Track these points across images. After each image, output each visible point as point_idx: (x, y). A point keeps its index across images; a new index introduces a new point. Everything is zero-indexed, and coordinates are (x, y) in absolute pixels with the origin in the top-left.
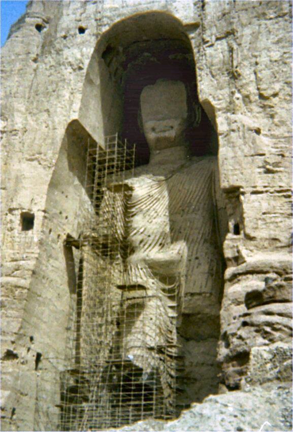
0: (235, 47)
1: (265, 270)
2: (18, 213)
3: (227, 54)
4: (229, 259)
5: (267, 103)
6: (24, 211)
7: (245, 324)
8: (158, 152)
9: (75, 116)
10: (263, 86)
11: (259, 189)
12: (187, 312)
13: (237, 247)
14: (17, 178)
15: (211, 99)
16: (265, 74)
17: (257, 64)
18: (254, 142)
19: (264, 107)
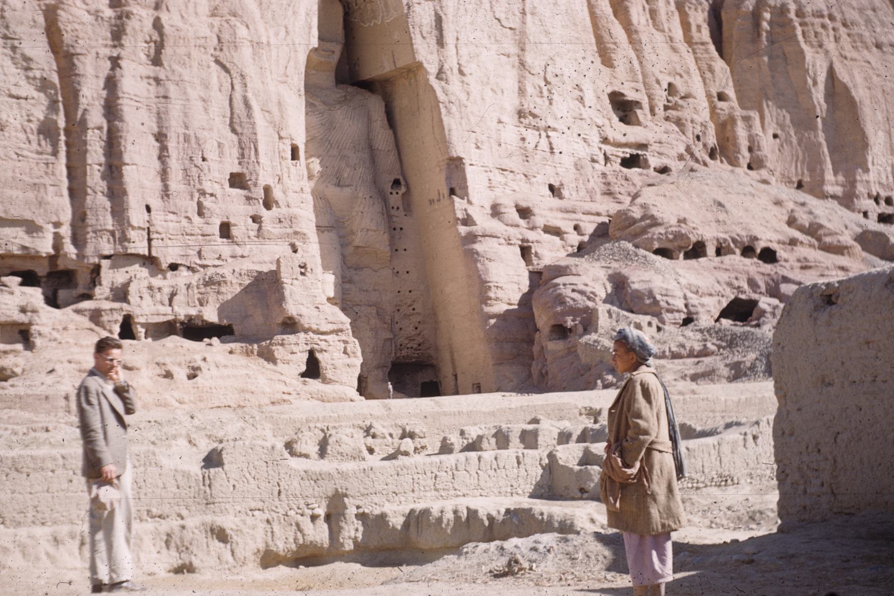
0: (443, 17)
1: (499, 235)
2: (288, 143)
3: (433, 18)
4: (458, 219)
5: (464, 79)
6: (294, 142)
7: (573, 291)
8: (314, 72)
9: (316, 46)
10: (462, 62)
11: (474, 163)
12: (360, 245)
13: (466, 210)
14: (279, 104)
15: (424, 62)
16: (463, 51)
17: (457, 39)
18: (468, 119)
19: (463, 82)
